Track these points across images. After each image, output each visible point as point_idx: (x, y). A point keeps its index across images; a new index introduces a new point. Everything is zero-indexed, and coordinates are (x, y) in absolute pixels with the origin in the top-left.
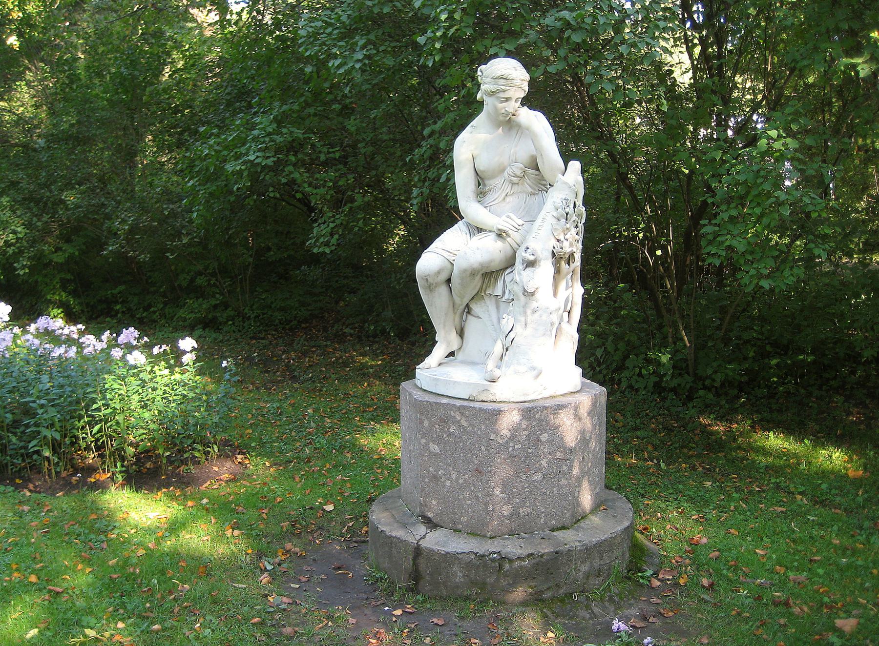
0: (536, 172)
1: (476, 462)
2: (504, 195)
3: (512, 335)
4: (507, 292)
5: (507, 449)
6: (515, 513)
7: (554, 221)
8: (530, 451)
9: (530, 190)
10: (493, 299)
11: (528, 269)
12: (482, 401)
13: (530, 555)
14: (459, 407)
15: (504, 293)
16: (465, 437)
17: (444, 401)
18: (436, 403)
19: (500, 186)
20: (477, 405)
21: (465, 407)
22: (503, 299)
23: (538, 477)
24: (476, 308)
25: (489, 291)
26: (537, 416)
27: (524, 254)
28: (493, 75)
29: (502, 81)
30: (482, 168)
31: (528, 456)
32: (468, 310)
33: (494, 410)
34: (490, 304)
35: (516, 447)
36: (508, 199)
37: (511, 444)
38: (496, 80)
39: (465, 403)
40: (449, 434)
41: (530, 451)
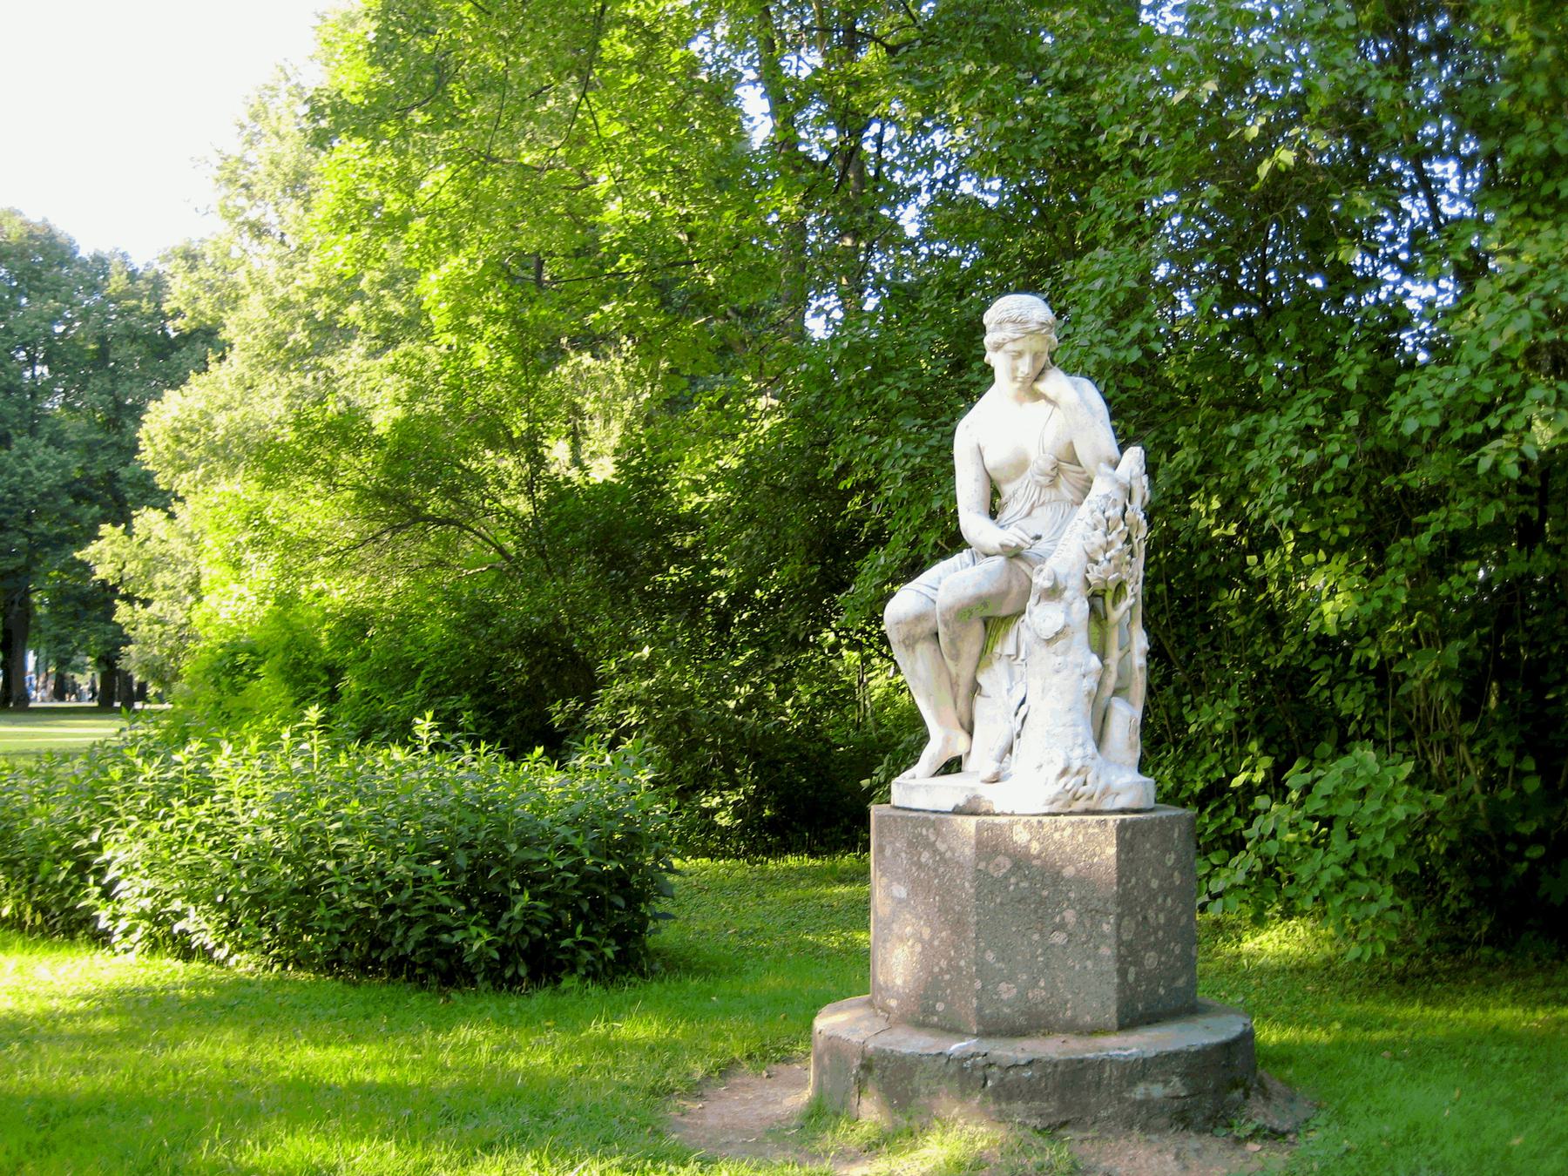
1: (957, 908)
2: (1028, 506)
5: (1007, 887)
6: (1022, 995)
8: (1045, 893)
10: (1005, 660)
13: (1030, 1063)
16: (941, 870)
23: (1059, 938)
24: (981, 679)
25: (997, 649)
29: (1009, 326)
31: (1042, 902)
32: (976, 688)
34: (999, 668)
35: (1022, 885)
36: (1035, 513)
37: (1013, 880)
40: (920, 866)
41: (1045, 893)
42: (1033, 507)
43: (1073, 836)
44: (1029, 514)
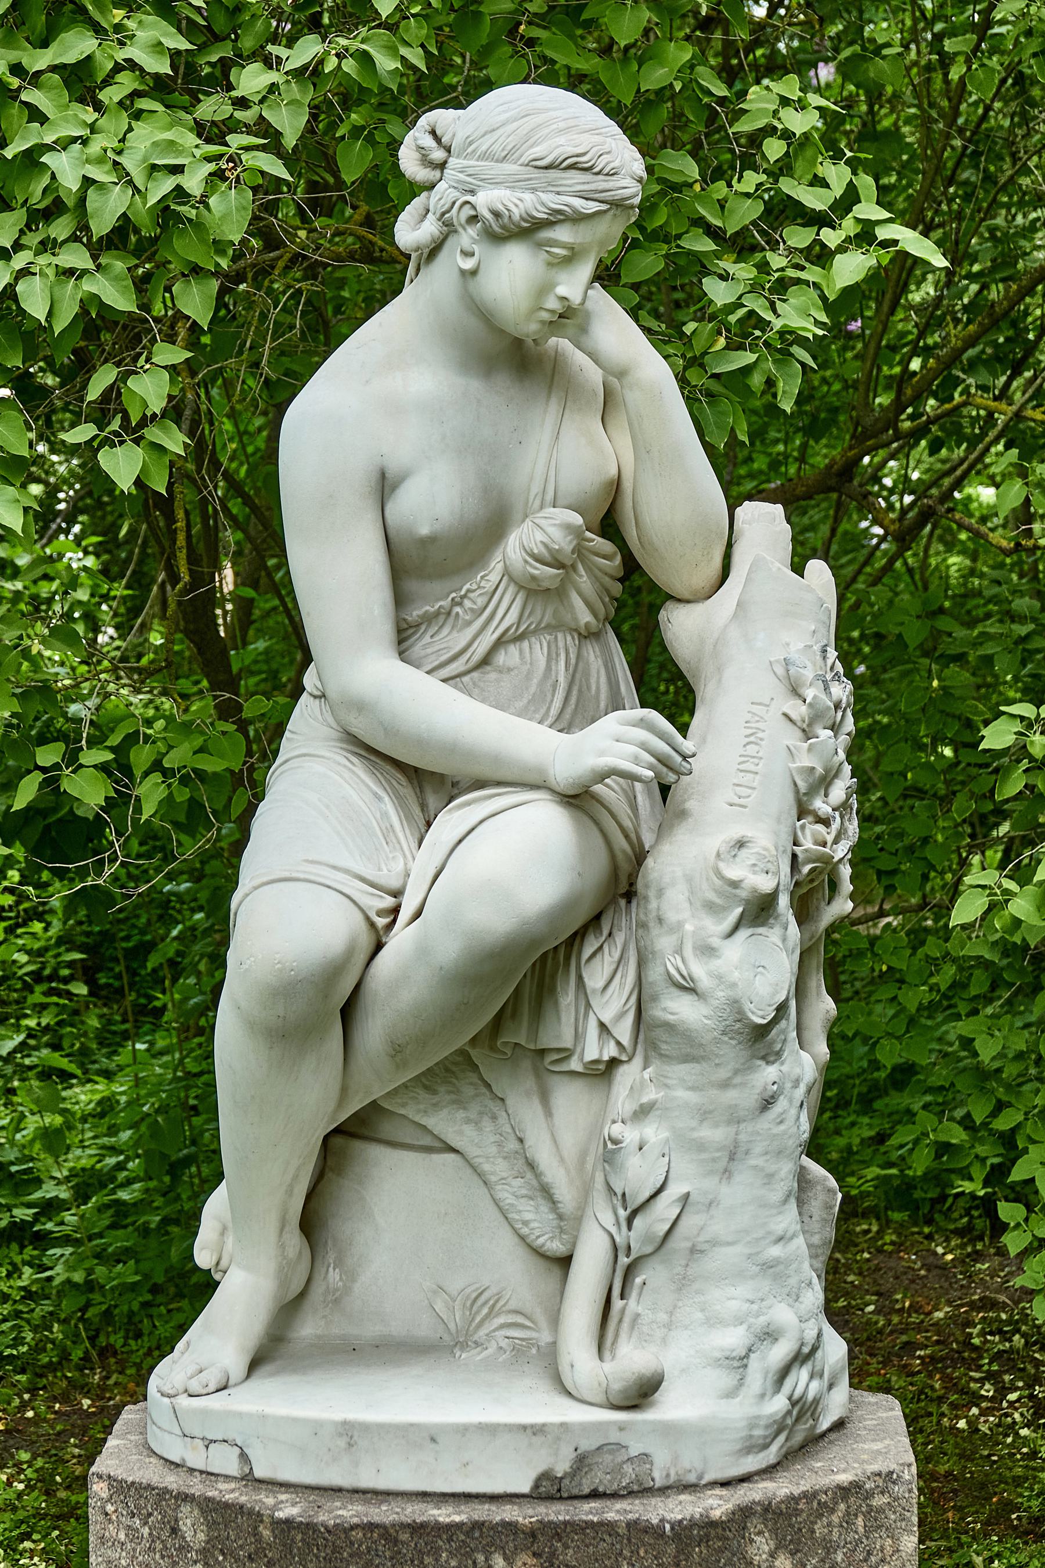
0: (606, 546)
3: (665, 1209)
4: (592, 1031)
7: (792, 737)
9: (585, 617)
11: (743, 934)
12: (595, 1495)
14: (533, 1534)
15: (579, 1036)
17: (445, 1515)
18: (417, 1529)
19: (481, 602)
20: (615, 1512)
21: (558, 1531)
22: (575, 1065)
26: (819, 1529)
27: (733, 873)
28: (537, 151)
29: (575, 180)
30: (424, 530)
33: (693, 1523)
38: (553, 174)
39: (557, 1513)
42: (499, 643)
43: (848, 1520)
44: (485, 661)
